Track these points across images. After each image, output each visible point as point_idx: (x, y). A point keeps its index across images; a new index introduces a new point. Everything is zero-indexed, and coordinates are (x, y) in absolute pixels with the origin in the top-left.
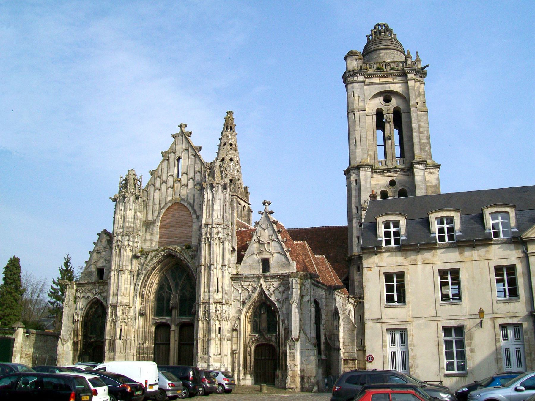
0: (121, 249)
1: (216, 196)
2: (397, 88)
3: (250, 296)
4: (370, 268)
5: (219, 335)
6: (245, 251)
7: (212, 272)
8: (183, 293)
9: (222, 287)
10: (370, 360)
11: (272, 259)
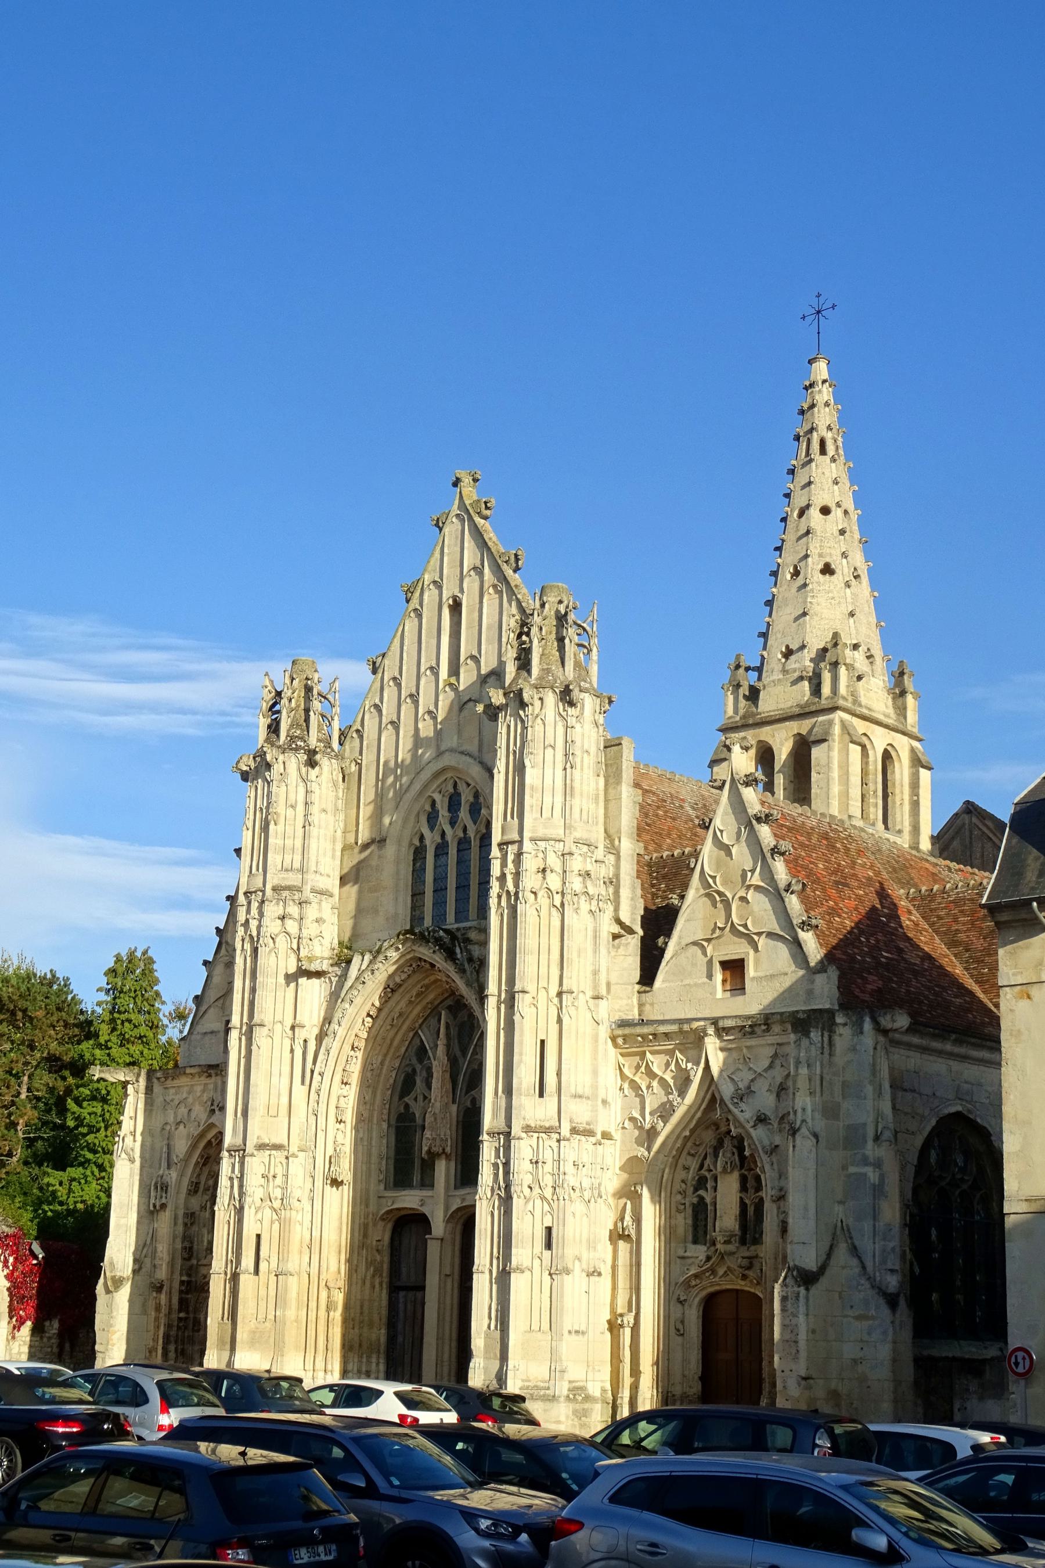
1: (536, 731)
4: (1025, 989)
5: (547, 1254)
6: (668, 934)
7: (517, 1018)
9: (559, 1074)
10: (1020, 1369)
11: (757, 962)
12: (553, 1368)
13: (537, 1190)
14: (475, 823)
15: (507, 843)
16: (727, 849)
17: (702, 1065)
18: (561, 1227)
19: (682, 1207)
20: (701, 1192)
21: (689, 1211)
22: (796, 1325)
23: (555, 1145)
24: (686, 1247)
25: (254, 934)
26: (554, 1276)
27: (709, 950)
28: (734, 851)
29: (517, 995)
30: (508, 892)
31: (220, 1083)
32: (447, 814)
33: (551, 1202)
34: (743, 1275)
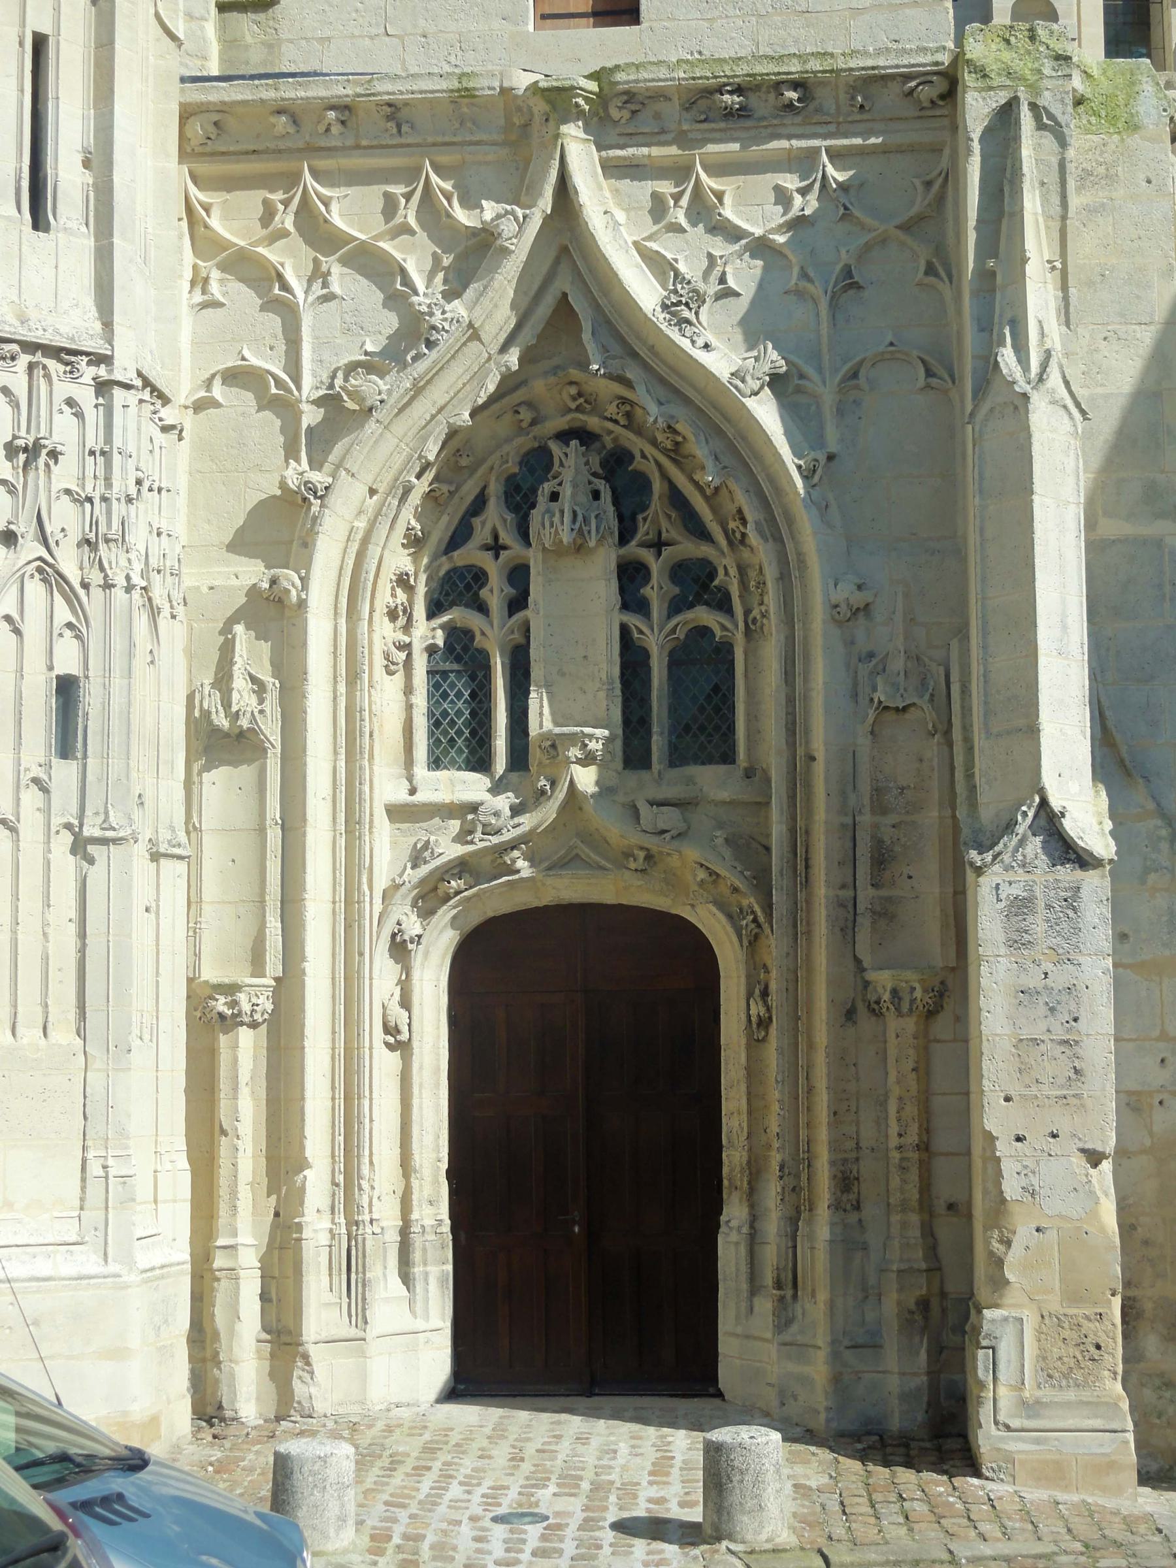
5: (65, 773)
12: (95, 1169)
13: (30, 549)
17: (546, 203)
18: (117, 682)
19: (402, 656)
21: (420, 664)
23: (86, 397)
24: (410, 779)
26: (91, 849)
33: (81, 592)
34: (649, 857)
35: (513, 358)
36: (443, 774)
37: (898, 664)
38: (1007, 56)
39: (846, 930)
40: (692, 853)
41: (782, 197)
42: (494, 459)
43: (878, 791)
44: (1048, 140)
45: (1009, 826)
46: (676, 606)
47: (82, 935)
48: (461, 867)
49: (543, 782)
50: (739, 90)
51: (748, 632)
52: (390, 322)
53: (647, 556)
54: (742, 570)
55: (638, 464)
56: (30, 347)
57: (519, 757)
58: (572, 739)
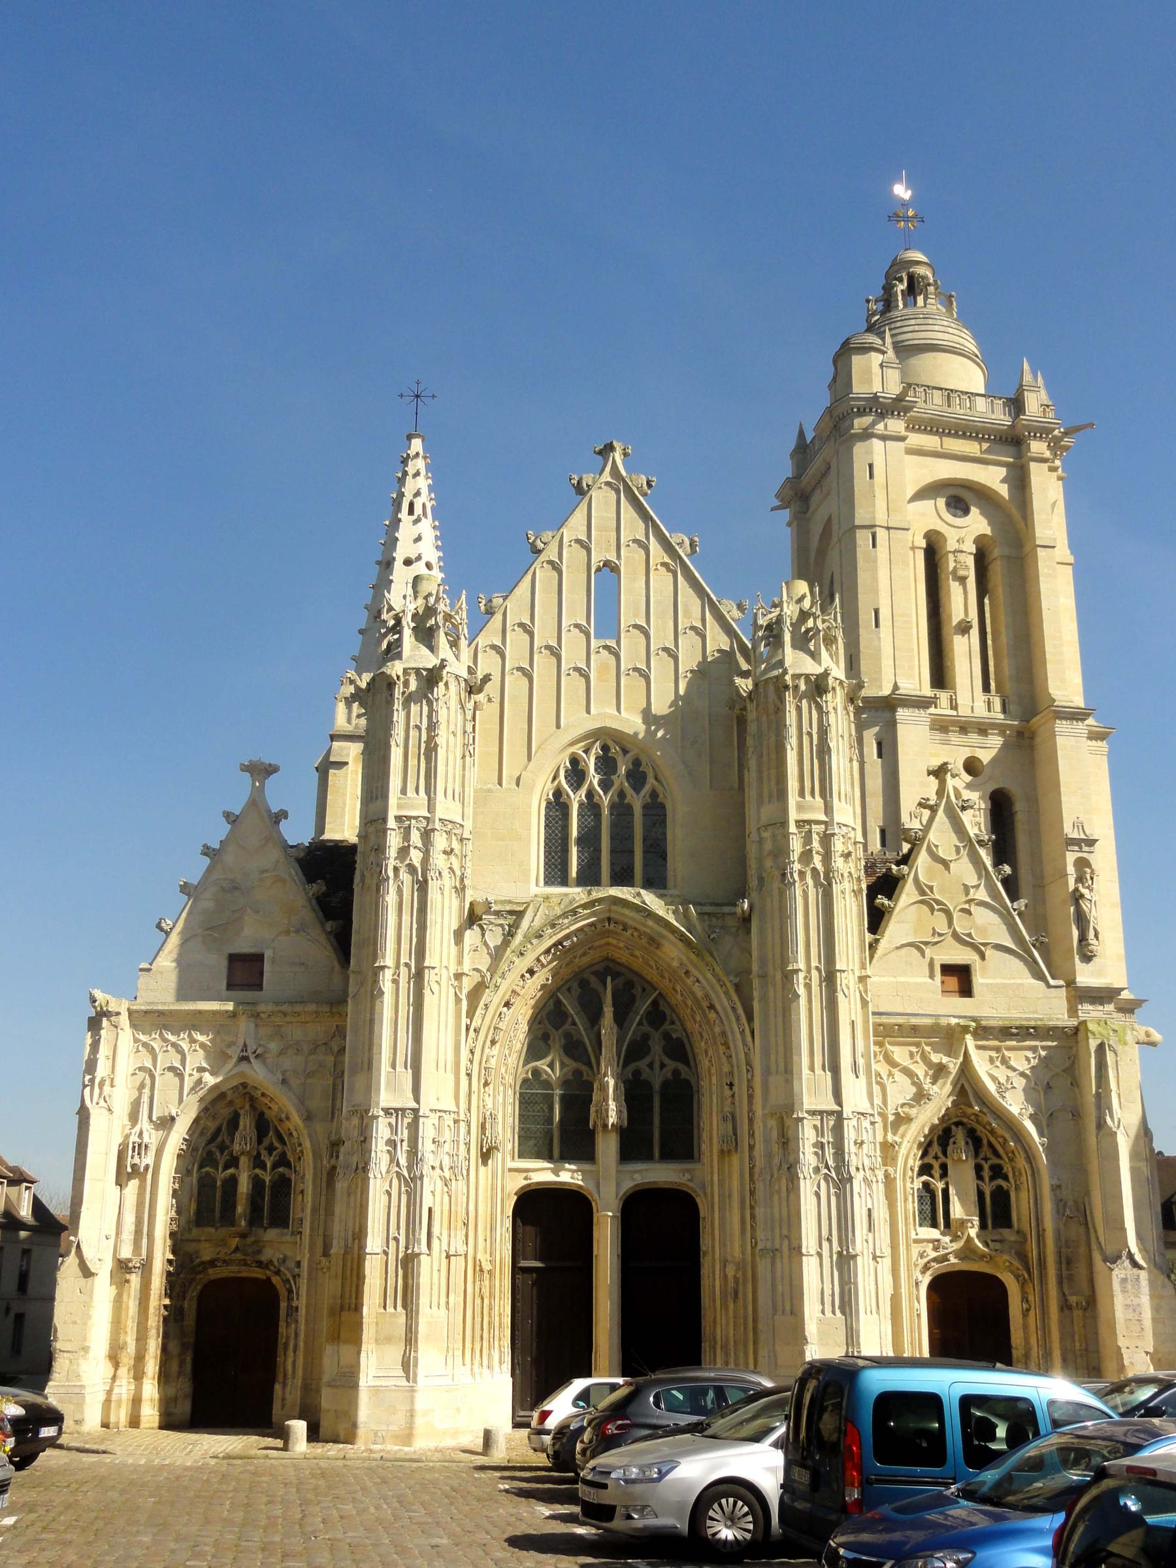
0: (426, 881)
2: (993, 477)
3: (921, 1096)
5: (871, 1235)
8: (637, 1073)
11: (983, 969)
14: (637, 790)
15: (809, 822)
16: (945, 864)
17: (961, 1059)
20: (925, 1178)
22: (1139, 1305)
25: (417, 864)
26: (878, 1259)
27: (928, 951)
28: (952, 865)
29: (838, 974)
30: (814, 870)
31: (252, 1026)
32: (597, 777)
35: (950, 1105)
36: (924, 1229)
37: (1070, 1203)
38: (1100, 1029)
39: (1060, 1282)
40: (1006, 1257)
41: (1028, 1059)
42: (936, 1131)
43: (1067, 1241)
44: (1112, 1053)
45: (1119, 1257)
46: (992, 1179)
47: (877, 1284)
48: (935, 1260)
49: (959, 1233)
50: (1016, 1028)
51: (1016, 1188)
52: (914, 1090)
53: (983, 1162)
54: (1013, 1169)
55: (979, 1133)
56: (858, 1113)
57: (948, 1224)
58: (969, 1221)
